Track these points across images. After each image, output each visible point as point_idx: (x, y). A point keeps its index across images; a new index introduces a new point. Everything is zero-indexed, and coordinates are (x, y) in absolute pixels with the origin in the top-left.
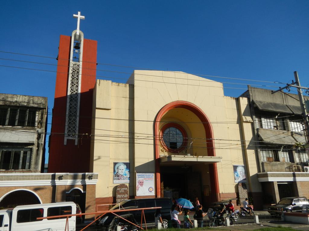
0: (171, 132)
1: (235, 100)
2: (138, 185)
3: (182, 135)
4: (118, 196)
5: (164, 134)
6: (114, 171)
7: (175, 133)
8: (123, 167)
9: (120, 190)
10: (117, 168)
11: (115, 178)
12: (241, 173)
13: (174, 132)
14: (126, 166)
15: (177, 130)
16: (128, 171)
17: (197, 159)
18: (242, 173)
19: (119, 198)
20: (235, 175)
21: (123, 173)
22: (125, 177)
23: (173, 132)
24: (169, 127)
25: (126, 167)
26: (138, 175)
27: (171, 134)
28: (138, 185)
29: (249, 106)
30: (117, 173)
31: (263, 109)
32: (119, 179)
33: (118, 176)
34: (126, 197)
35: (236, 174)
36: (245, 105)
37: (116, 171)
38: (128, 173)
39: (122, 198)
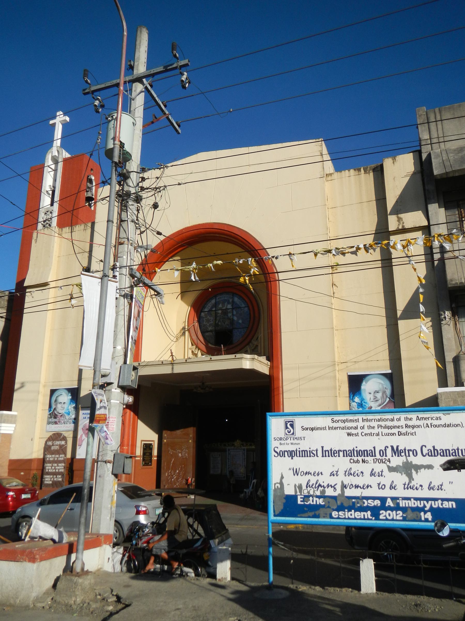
0: (220, 306)
1: (372, 174)
2: (82, 436)
3: (246, 309)
4: (48, 456)
5: (203, 314)
6: (50, 406)
7: (229, 306)
8: (65, 398)
9: (53, 445)
10: (56, 401)
11: (50, 420)
12: (375, 397)
13: (229, 303)
14: (72, 395)
15: (236, 299)
16: (74, 405)
17: (173, 368)
18: (379, 396)
19: (50, 462)
20: (354, 404)
21: (65, 409)
22: (67, 417)
23: (226, 304)
24: (215, 296)
25: (71, 397)
26: (83, 414)
27: (220, 312)
28: (82, 436)
29: (419, 176)
30: (54, 411)
31: (447, 173)
32: (56, 423)
33: (55, 417)
34: (62, 459)
35: (357, 399)
36: (405, 176)
37: (53, 407)
38: (73, 409)
39: (54, 462)
